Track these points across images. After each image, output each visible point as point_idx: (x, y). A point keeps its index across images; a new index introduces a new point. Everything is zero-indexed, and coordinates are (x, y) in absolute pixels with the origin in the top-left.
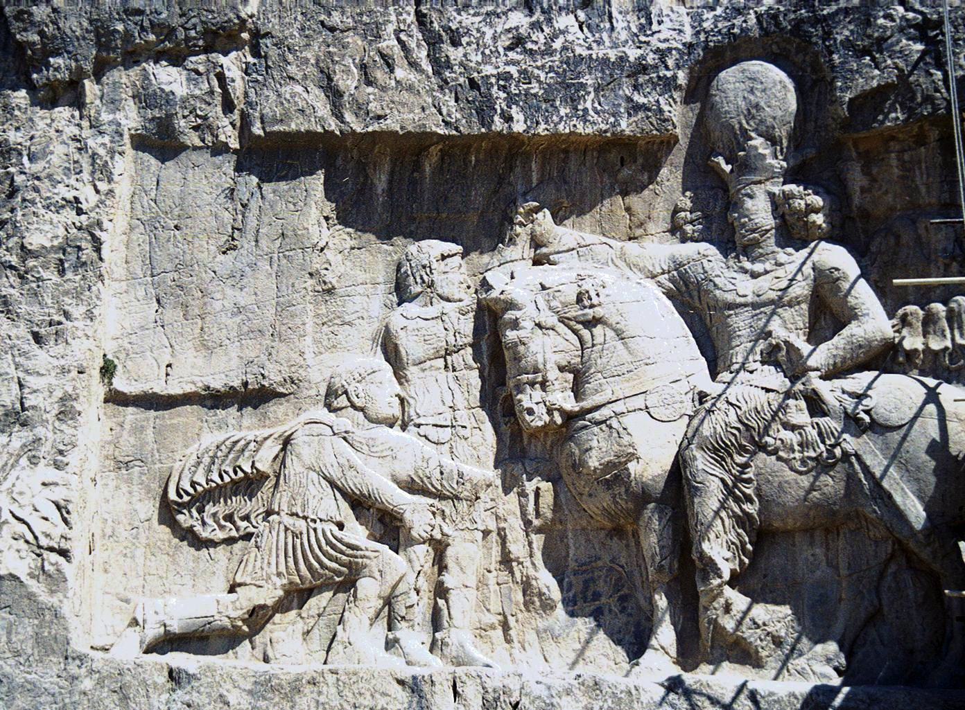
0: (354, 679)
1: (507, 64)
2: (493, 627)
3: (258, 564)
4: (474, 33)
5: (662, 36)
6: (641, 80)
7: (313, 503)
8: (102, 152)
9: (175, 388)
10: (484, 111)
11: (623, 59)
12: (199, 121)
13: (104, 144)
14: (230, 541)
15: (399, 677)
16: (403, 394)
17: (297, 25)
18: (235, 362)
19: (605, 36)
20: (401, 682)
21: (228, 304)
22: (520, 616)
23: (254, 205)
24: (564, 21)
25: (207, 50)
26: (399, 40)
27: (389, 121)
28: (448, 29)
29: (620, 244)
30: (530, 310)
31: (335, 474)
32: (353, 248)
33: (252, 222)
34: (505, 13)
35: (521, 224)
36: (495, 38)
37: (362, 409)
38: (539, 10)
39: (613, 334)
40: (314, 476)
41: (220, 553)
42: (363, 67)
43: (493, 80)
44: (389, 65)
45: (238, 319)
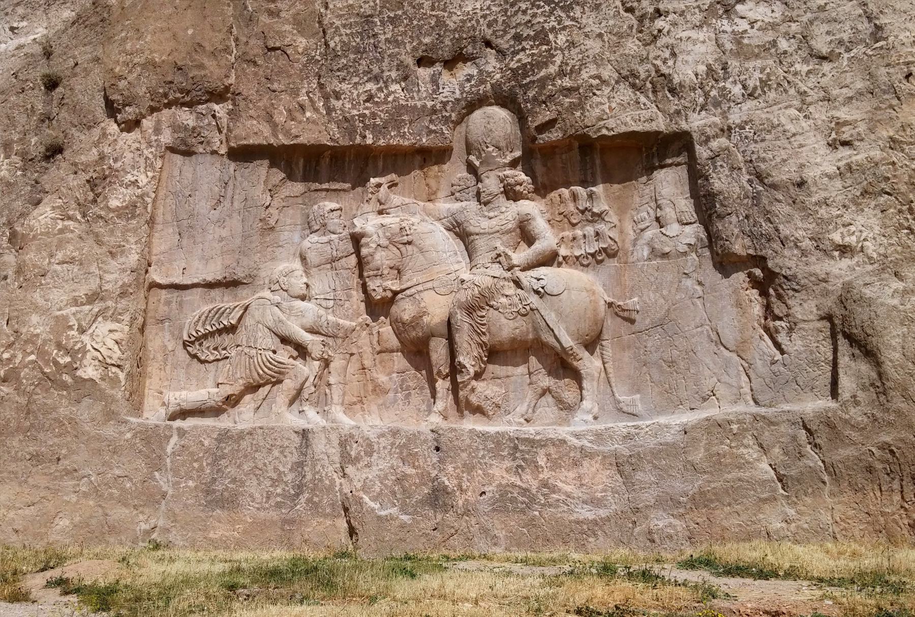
0: (272, 431)
1: (365, 109)
2: (355, 404)
3: (231, 373)
4: (348, 93)
5: (444, 95)
6: (433, 118)
7: (260, 341)
8: (150, 156)
9: (189, 282)
10: (352, 132)
11: (424, 106)
12: (203, 139)
13: (152, 152)
14: (218, 360)
15: (296, 430)
16: (309, 283)
17: (255, 89)
18: (219, 267)
19: (415, 94)
20: (296, 432)
21: (217, 236)
22: (369, 398)
23: (231, 183)
24: (394, 87)
25: (207, 101)
26: (308, 96)
27: (302, 138)
28: (334, 91)
29: (422, 204)
30: (375, 237)
31: (271, 324)
32: (284, 207)
33: (230, 192)
34: (364, 83)
35: (372, 193)
36: (358, 95)
37: (286, 291)
38: (382, 81)
39: (417, 250)
40: (260, 326)
41: (211, 367)
42: (289, 111)
43: (357, 118)
44: (303, 110)
45: (221, 244)
